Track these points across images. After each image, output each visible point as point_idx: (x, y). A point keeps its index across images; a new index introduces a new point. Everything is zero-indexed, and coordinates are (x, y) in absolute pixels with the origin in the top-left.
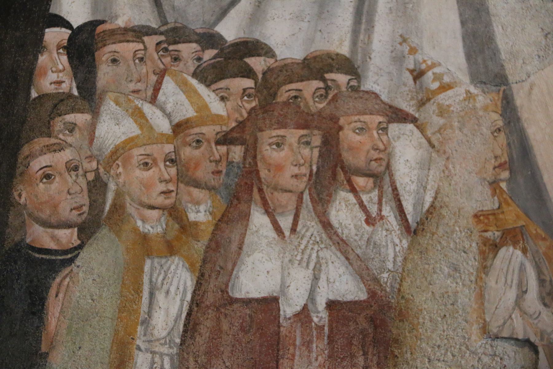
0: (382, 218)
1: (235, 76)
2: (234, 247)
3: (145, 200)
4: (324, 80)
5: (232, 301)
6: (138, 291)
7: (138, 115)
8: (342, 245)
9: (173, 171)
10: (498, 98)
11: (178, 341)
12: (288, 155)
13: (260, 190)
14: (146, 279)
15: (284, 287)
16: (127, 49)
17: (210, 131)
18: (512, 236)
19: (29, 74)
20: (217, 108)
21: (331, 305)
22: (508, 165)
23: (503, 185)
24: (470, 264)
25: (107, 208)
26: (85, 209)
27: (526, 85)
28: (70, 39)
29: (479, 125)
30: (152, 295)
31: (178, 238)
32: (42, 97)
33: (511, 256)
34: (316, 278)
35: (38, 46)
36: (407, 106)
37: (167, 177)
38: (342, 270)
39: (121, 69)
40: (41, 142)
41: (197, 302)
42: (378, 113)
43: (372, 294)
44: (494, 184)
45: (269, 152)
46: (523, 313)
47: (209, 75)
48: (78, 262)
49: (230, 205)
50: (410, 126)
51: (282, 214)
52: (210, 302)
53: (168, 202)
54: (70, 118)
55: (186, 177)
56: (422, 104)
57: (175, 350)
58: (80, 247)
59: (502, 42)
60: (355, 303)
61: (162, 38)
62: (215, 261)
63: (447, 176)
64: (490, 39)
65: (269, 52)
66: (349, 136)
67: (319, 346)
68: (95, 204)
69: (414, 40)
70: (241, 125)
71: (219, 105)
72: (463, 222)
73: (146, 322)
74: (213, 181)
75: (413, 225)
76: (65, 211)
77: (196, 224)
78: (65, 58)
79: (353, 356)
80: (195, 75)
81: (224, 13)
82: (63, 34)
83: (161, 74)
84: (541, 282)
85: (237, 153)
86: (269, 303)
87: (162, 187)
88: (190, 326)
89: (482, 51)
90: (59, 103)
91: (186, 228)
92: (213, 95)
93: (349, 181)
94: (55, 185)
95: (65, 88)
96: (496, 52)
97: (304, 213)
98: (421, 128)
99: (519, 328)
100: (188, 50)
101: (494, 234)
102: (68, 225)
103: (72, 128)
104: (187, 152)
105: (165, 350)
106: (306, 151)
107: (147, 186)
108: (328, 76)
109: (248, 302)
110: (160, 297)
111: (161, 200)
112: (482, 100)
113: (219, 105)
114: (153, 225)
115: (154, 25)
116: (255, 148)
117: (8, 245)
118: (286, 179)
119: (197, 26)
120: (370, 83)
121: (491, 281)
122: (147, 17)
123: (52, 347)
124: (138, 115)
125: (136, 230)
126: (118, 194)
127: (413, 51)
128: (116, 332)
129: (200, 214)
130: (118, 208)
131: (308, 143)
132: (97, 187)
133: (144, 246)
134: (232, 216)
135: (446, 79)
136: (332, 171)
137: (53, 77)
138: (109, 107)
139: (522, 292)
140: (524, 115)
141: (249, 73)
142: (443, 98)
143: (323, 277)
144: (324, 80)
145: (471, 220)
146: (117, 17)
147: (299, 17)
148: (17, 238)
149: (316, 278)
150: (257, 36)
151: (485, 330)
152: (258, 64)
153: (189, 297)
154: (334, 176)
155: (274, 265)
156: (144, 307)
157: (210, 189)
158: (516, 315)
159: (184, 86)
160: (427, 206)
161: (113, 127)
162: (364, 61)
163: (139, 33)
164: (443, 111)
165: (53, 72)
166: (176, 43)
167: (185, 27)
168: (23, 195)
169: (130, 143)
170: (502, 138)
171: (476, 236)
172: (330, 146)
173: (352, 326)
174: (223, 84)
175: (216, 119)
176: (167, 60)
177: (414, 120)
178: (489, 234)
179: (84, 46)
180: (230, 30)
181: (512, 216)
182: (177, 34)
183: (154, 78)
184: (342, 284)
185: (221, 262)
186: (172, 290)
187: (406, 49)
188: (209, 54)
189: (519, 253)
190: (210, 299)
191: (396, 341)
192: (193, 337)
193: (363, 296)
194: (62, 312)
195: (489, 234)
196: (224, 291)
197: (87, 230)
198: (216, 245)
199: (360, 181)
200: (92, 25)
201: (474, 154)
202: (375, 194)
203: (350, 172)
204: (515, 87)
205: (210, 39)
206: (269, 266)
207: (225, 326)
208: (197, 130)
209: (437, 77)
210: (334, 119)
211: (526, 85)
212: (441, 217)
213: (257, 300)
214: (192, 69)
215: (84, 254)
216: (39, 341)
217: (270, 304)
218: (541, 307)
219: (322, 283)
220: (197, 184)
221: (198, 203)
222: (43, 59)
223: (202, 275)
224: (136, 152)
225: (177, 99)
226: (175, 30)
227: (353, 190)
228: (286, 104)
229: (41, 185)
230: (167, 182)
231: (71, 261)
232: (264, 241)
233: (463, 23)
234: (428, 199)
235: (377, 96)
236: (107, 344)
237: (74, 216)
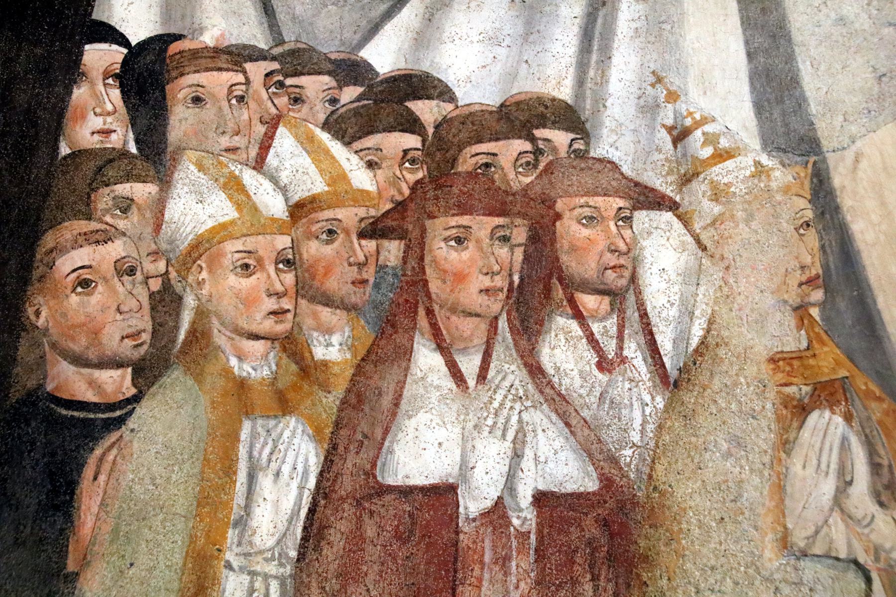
0: (623, 360)
1: (390, 129)
2: (386, 401)
3: (244, 324)
4: (532, 139)
5: (383, 490)
6: (230, 471)
7: (234, 188)
8: (559, 403)
9: (289, 278)
10: (805, 173)
11: (293, 554)
12: (471, 259)
13: (430, 312)
14: (243, 452)
15: (465, 468)
16: (217, 81)
17: (349, 216)
18: (828, 393)
19: (57, 117)
20: (362, 179)
21: (541, 499)
22: (823, 281)
23: (815, 312)
24: (764, 437)
25: (182, 336)
26: (146, 337)
27: (850, 155)
28: (125, 62)
29: (776, 216)
30: (252, 478)
31: (295, 387)
32: (77, 155)
33: (826, 427)
34: (517, 455)
35: (73, 70)
37: (279, 288)
38: (558, 443)
39: (208, 112)
41: (324, 493)
42: (617, 193)
43: (607, 482)
44: (801, 310)
45: (442, 252)
46: (847, 516)
47: (348, 127)
48: (132, 423)
49: (381, 334)
50: (668, 216)
51: (464, 350)
52: (348, 490)
53: (281, 328)
54: (124, 189)
56: (686, 180)
57: (288, 570)
58: (136, 399)
59: (813, 84)
60: (578, 496)
61: (275, 66)
63: (726, 296)
64: (795, 81)
65: (445, 93)
66: (571, 230)
67: (522, 565)
68: (162, 329)
69: (674, 81)
70: (400, 207)
71: (365, 174)
72: (751, 370)
73: (242, 523)
74: (356, 296)
75: (673, 374)
76: (113, 340)
77: (325, 364)
78: (116, 94)
79: (575, 582)
80: (326, 126)
81: (374, 29)
82: (115, 54)
83: (273, 124)
84: (875, 468)
85: (393, 251)
86: (440, 494)
87: (271, 304)
88: (314, 531)
89: (780, 101)
90: (105, 165)
91: (309, 371)
92: (355, 159)
93: (572, 302)
95: (115, 141)
96: (801, 103)
97: (498, 351)
98: (685, 220)
99: (839, 537)
100: (315, 85)
101: (800, 390)
102: (119, 365)
103: (125, 206)
104: (313, 249)
105: (272, 568)
106: (503, 252)
107: (248, 301)
108: (539, 133)
109: (406, 492)
110: (265, 482)
111: (269, 325)
112: (781, 176)
113: (365, 174)
114: (255, 364)
115: (262, 45)
116: (422, 245)
117: (15, 395)
118: (471, 294)
119: (331, 48)
120: (602, 149)
122: (251, 32)
123: (85, 562)
124: (234, 188)
125: (227, 372)
126: (201, 313)
127: (672, 97)
128: (193, 539)
129: (332, 347)
130: (199, 335)
131: (505, 239)
132: (165, 301)
133: (240, 397)
134: (384, 351)
135: (724, 143)
137: (97, 123)
138: (187, 173)
139: (845, 483)
140: (846, 202)
141: (412, 125)
142: (720, 173)
143: (529, 453)
144: (532, 139)
145: (766, 369)
146: (201, 30)
147: (494, 40)
148: (31, 384)
149: (517, 455)
150: (425, 66)
151: (784, 542)
152: (427, 111)
153: (312, 483)
154: (548, 291)
155: (451, 434)
156: (239, 499)
157: (349, 308)
158: (836, 517)
159: (309, 144)
160: (695, 342)
161: (195, 206)
162: (596, 112)
163: (236, 56)
164: (718, 194)
165: (97, 116)
166: (296, 74)
167: (312, 49)
168: (43, 312)
170: (812, 238)
171: (771, 394)
173: (575, 533)
174: (370, 141)
175: (360, 197)
176: (283, 101)
177: (673, 206)
178: (791, 390)
179: (148, 75)
180: (384, 55)
181: (830, 361)
182: (297, 61)
183: (260, 130)
184: (560, 466)
185: (364, 427)
186: (283, 474)
187: (662, 94)
188: (350, 94)
189: (839, 420)
190: (346, 485)
191: (645, 558)
192: (317, 548)
193: (592, 485)
194: (103, 504)
195: (791, 390)
196: (370, 474)
197: (147, 372)
198: (356, 399)
199: (589, 301)
201: (771, 258)
202: (612, 323)
203: (573, 286)
204: (831, 158)
205: (352, 70)
206: (441, 434)
207: (370, 531)
208: (328, 214)
209: (710, 139)
210: (548, 202)
211: (850, 155)
212: (716, 359)
213: (423, 489)
214: (322, 117)
215: (142, 410)
216: (63, 553)
217: (443, 495)
218: (874, 508)
219: (527, 463)
220: (328, 301)
221: (329, 331)
222: (80, 93)
223: (335, 447)
224: (231, 247)
225: (298, 163)
226: (293, 53)
227: (578, 315)
228: (472, 175)
229: (74, 299)
230: (279, 295)
231: (120, 421)
232: (435, 395)
233: (750, 56)
234: (697, 332)
235: (614, 166)
236: (178, 559)
237: (126, 349)
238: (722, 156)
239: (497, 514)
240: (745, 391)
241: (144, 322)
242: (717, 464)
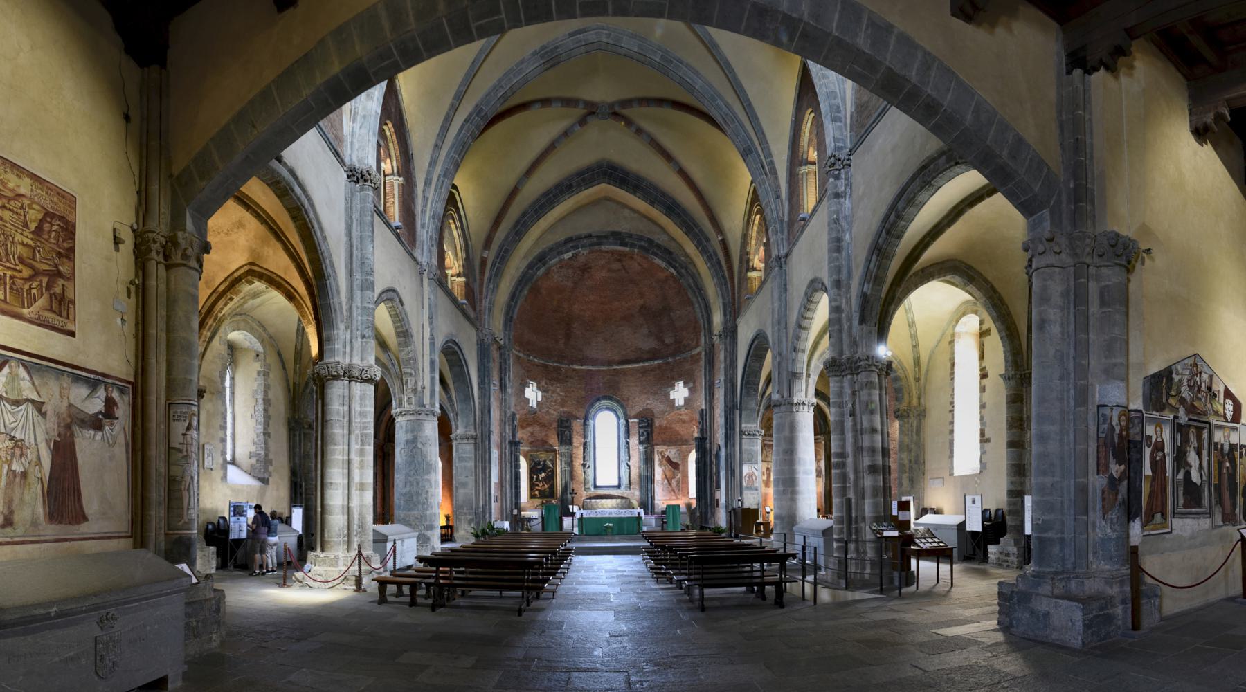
52: (9, 470)
71: (11, 444)
136: (22, 455)
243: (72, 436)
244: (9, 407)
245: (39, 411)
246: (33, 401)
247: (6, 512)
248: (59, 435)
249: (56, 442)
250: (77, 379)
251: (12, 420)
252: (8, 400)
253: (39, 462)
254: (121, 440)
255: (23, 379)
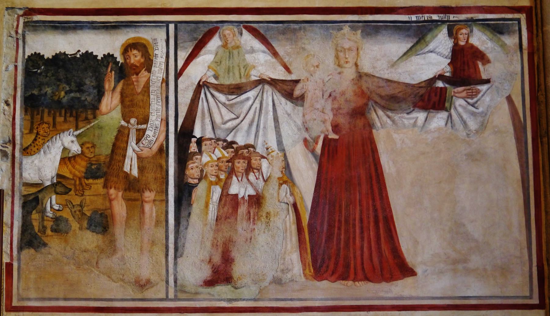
5: (229, 195)
6: (210, 192)
7: (210, 156)
8: (251, 184)
10: (283, 154)
12: (240, 165)
15: (239, 192)
17: (225, 160)
18: (285, 182)
19: (188, 148)
20: (226, 155)
21: (249, 196)
22: (285, 168)
24: (277, 187)
32: (191, 152)
33: (285, 186)
35: (190, 142)
36: (265, 155)
39: (207, 146)
40: (191, 162)
41: (222, 195)
43: (257, 194)
44: (282, 172)
45: (237, 164)
47: (225, 148)
52: (225, 195)
53: (216, 174)
54: (197, 157)
55: (220, 169)
56: (268, 155)
59: (284, 142)
62: (225, 187)
63: (272, 170)
64: (282, 142)
65: (237, 143)
66: (253, 161)
67: (246, 204)
68: (202, 175)
69: (267, 142)
70: (231, 159)
71: (227, 154)
73: (212, 198)
74: (225, 170)
76: (196, 176)
81: (228, 135)
82: (196, 139)
83: (215, 148)
84: (290, 191)
85: (230, 164)
88: (221, 199)
90: (194, 154)
91: (220, 180)
94: (194, 170)
95: (195, 151)
96: (283, 145)
98: (268, 160)
100: (220, 143)
101: (281, 182)
103: (197, 159)
104: (220, 164)
107: (212, 171)
109: (232, 195)
110: (214, 193)
112: (280, 154)
113: (227, 154)
114: (213, 179)
118: (240, 170)
120: (257, 150)
121: (280, 191)
122: (212, 136)
123: (193, 202)
124: (210, 156)
126: (206, 172)
127: (266, 144)
130: (206, 175)
132: (202, 171)
133: (211, 183)
136: (249, 169)
137: (193, 148)
138: (204, 155)
139: (286, 193)
140: (288, 158)
141: (233, 148)
142: (272, 154)
147: (243, 136)
151: (279, 201)
159: (220, 150)
161: (205, 158)
163: (211, 139)
164: (272, 156)
165: (193, 147)
169: (209, 162)
172: (249, 163)
175: (226, 157)
177: (266, 158)
179: (200, 142)
180: (229, 139)
181: (285, 178)
182: (218, 140)
184: (252, 192)
186: (217, 192)
188: (225, 144)
190: (224, 194)
193: (255, 194)
196: (227, 192)
197: (200, 180)
198: (226, 183)
199: (255, 171)
200: (201, 137)
203: (253, 169)
205: (225, 141)
209: (271, 149)
210: (250, 158)
215: (199, 185)
216: (191, 201)
217: (236, 195)
219: (247, 191)
220: (222, 171)
222: (191, 145)
224: (210, 164)
225: (218, 153)
227: (254, 173)
237: (197, 177)
238: (273, 152)
239: (243, 198)
240: (275, 182)
241: (199, 174)
242: (271, 191)
243: (370, 126)
244: (222, 98)
245: (289, 95)
246: (273, 83)
247: (217, 259)
248: (336, 128)
249: (327, 141)
250: (372, 30)
251: (228, 115)
252: (219, 88)
253: (287, 177)
254: (503, 119)
255: (253, 51)
